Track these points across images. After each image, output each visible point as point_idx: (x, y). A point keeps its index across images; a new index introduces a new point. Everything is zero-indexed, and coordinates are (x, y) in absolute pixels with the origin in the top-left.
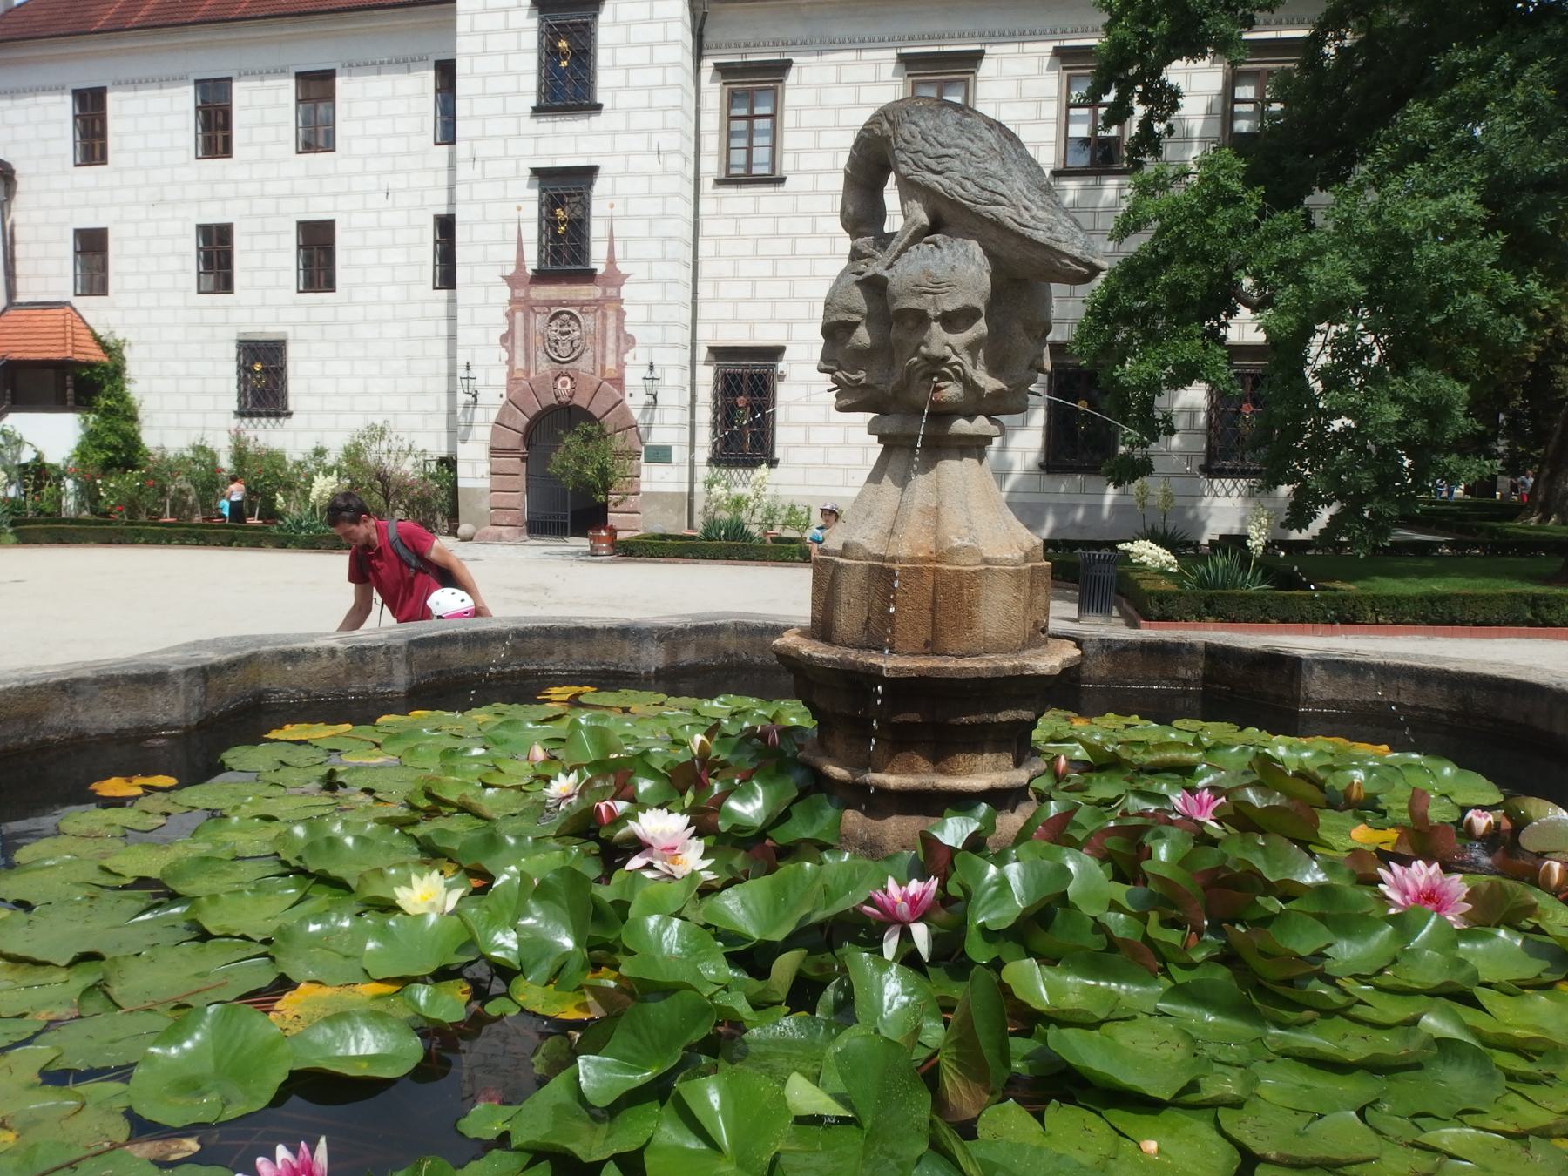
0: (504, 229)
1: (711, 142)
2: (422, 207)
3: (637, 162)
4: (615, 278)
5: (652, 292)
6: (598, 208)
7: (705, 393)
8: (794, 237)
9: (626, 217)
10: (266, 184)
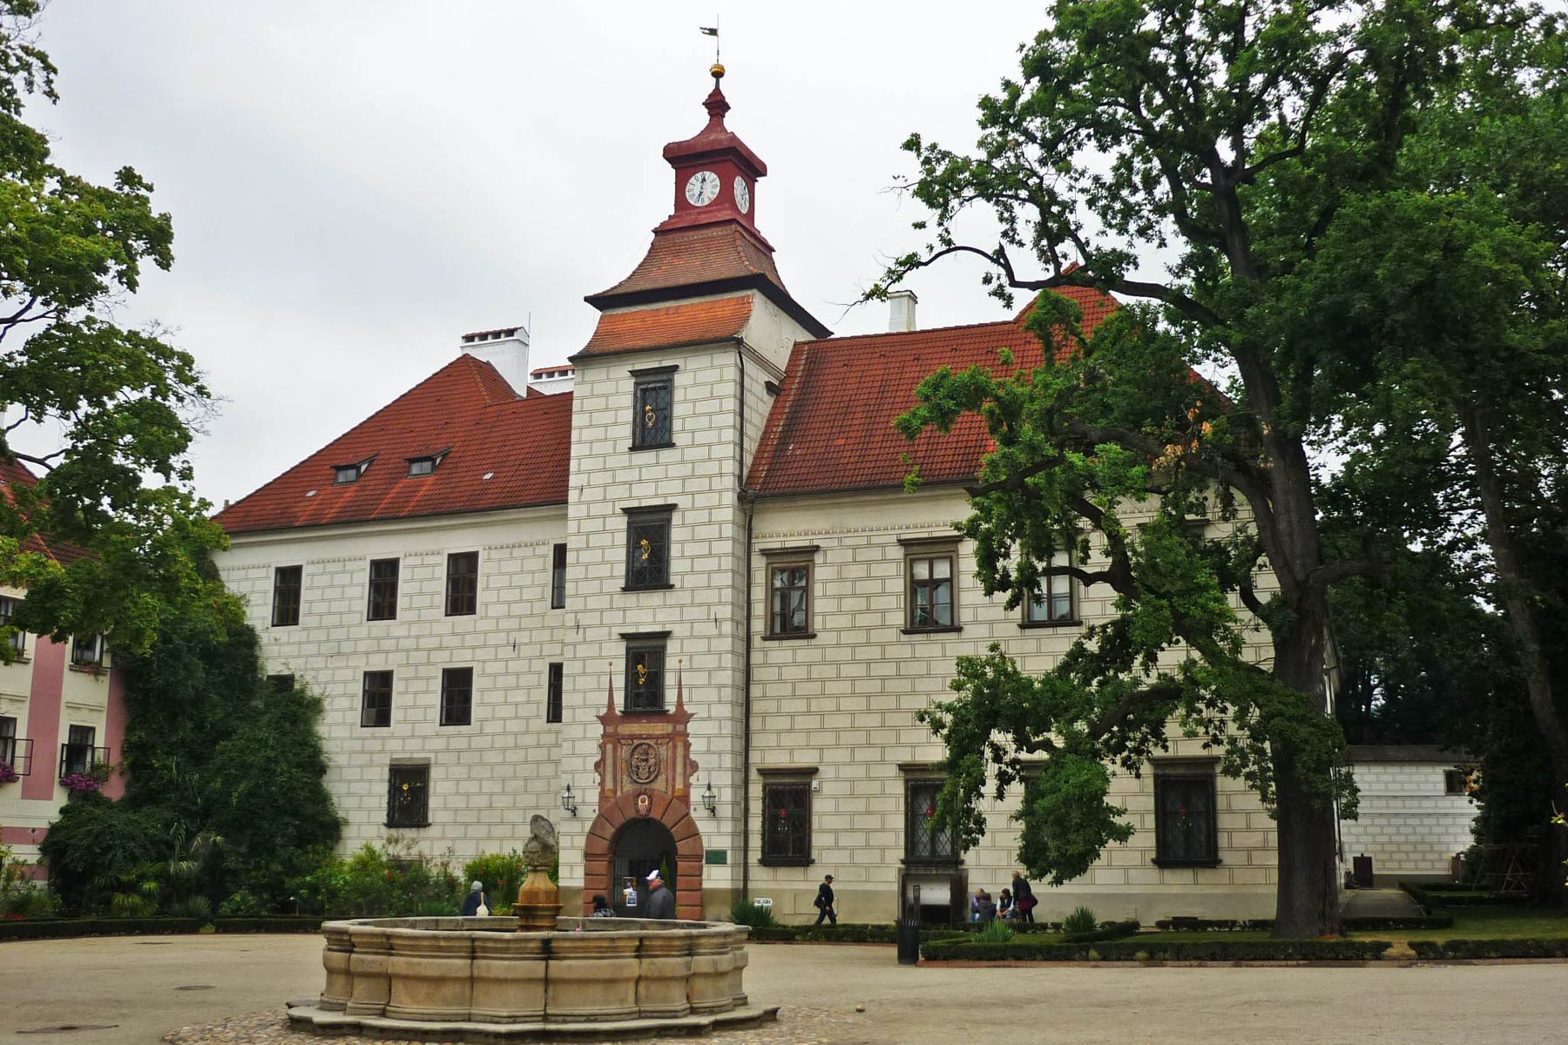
0: (599, 681)
1: (759, 609)
2: (541, 657)
3: (700, 629)
4: (682, 717)
5: (710, 728)
6: (671, 663)
7: (756, 807)
8: (823, 681)
9: (691, 670)
10: (422, 638)
